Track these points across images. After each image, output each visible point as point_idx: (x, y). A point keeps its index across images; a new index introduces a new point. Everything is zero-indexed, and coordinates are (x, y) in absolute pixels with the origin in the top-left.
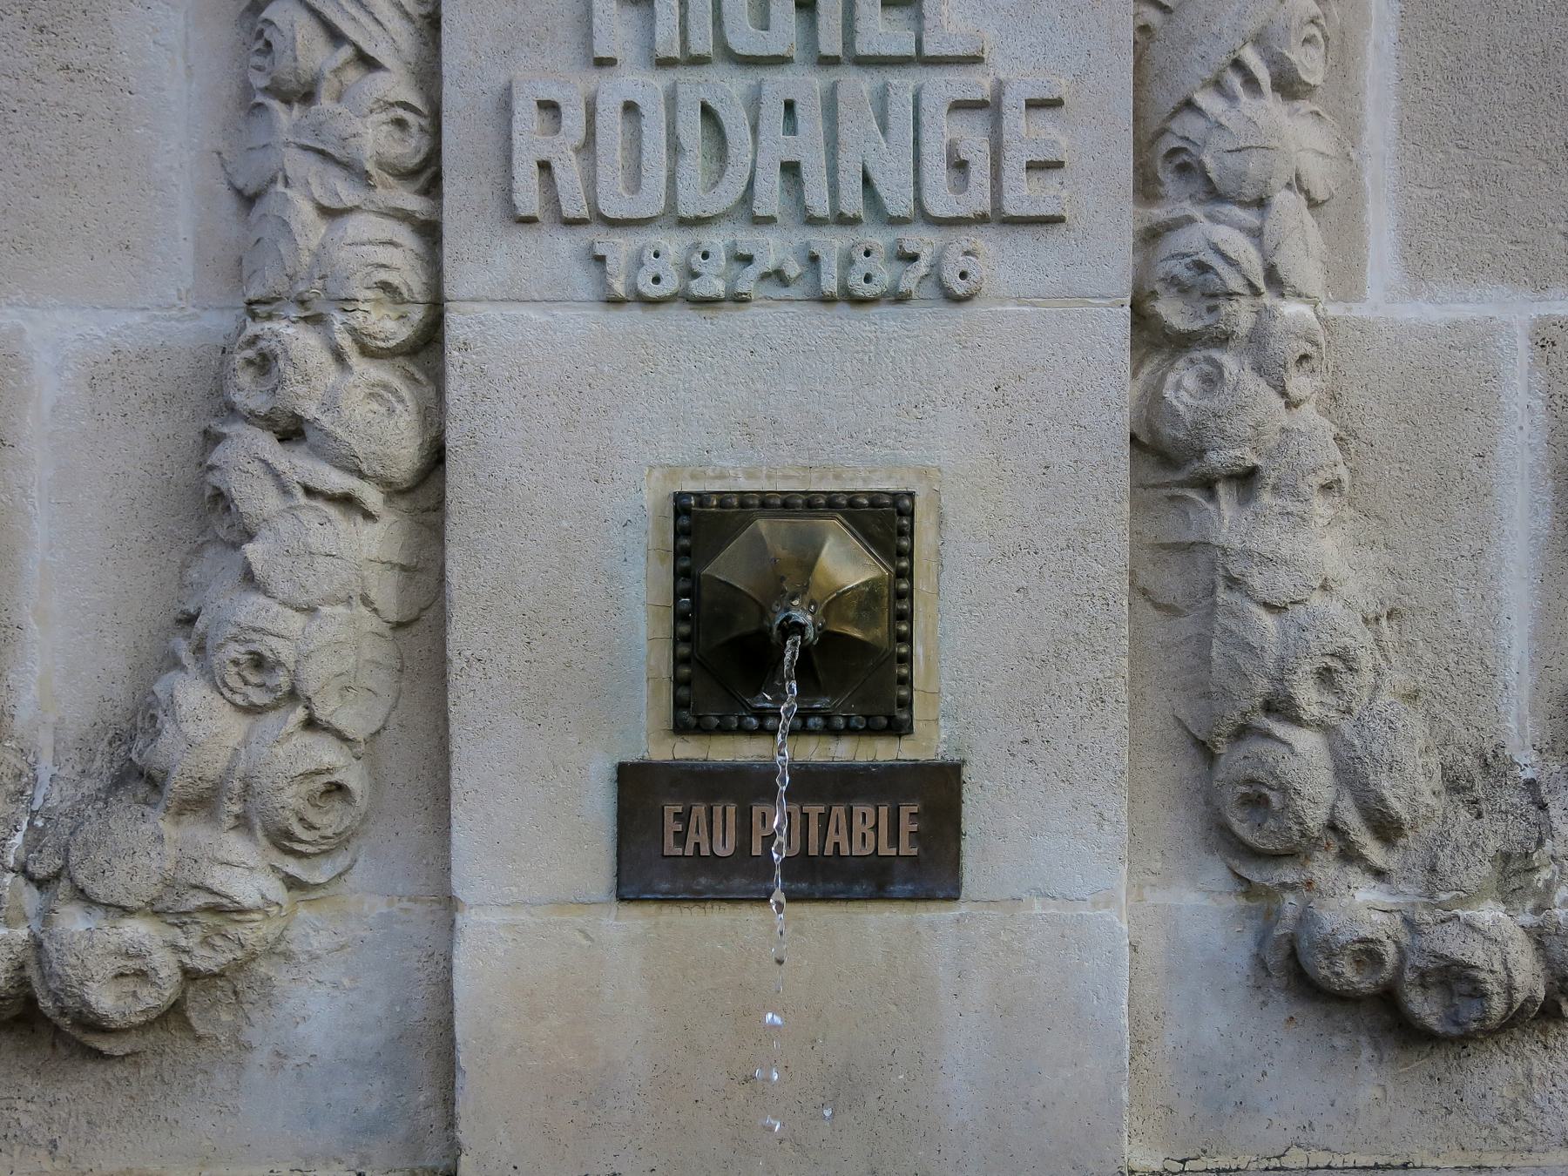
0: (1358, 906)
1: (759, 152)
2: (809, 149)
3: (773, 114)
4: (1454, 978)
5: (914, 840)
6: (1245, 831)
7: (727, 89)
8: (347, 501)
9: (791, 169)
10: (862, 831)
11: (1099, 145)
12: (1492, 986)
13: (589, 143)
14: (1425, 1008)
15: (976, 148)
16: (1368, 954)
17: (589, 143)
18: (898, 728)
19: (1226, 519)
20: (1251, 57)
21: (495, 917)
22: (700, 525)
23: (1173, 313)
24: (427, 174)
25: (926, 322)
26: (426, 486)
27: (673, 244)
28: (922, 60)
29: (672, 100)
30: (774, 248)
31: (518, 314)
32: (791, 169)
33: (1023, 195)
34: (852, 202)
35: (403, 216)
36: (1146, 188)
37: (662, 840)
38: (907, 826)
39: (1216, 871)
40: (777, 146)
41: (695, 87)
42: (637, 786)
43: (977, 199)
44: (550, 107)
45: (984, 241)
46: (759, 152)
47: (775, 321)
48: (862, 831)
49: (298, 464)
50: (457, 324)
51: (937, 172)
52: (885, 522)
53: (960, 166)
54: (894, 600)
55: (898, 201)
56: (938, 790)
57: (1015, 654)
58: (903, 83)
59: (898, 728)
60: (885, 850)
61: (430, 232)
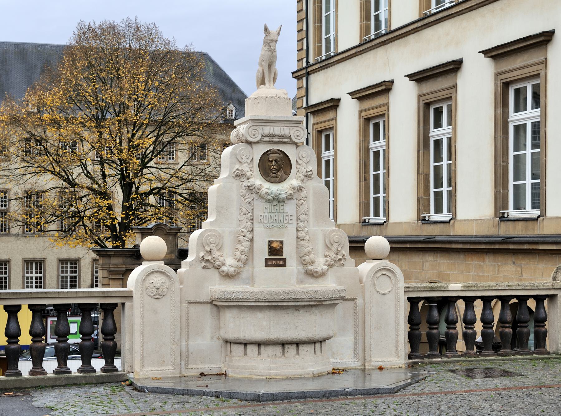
0: (311, 267)
4: (317, 272)
6: (304, 263)
7: (272, 214)
10: (280, 262)
14: (315, 274)
16: (311, 270)
18: (282, 255)
19: (302, 242)
22: (270, 243)
23: (299, 229)
24: (252, 220)
25: (284, 229)
26: (252, 240)
27: (269, 224)
30: (275, 225)
31: (259, 229)
36: (297, 220)
37: (267, 263)
39: (302, 265)
41: (270, 214)
42: (266, 260)
47: (275, 229)
48: (280, 262)
49: (244, 238)
50: (255, 229)
52: (282, 242)
54: (282, 248)
56: (285, 260)
59: (282, 255)
61: (252, 223)
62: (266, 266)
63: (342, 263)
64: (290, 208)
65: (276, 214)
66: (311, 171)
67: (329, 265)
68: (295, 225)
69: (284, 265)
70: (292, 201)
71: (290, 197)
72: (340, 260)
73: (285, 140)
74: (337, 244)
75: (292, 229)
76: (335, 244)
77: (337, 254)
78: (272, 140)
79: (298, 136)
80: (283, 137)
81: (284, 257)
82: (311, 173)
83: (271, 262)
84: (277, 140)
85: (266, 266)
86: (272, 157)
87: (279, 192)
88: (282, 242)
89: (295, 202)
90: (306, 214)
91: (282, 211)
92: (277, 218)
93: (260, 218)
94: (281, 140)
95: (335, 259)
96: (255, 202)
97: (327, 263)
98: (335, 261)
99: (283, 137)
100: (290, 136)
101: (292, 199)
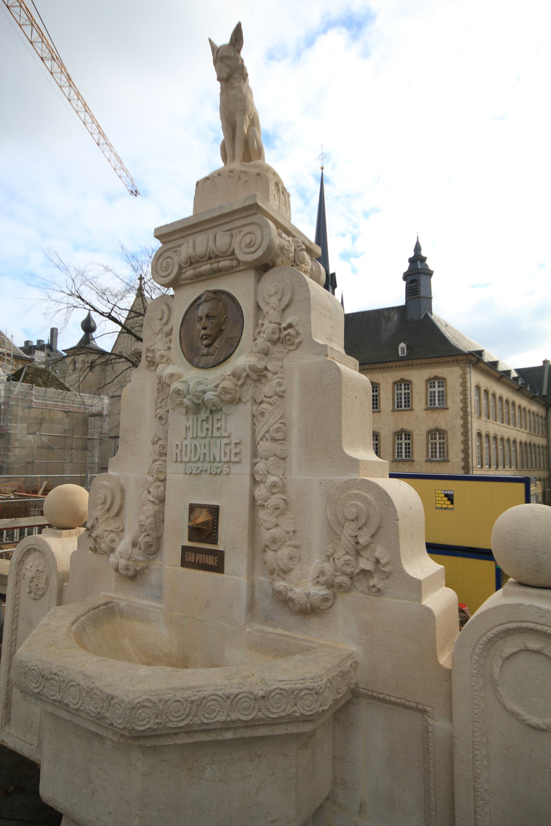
1: (201, 451)
2: (206, 451)
3: (203, 446)
5: (216, 564)
8: (153, 502)
9: (205, 454)
10: (211, 560)
11: (246, 450)
12: (297, 603)
13: (181, 451)
15: (227, 451)
17: (181, 451)
20: (267, 435)
21: (167, 567)
28: (221, 437)
29: (191, 444)
32: (205, 454)
33: (234, 459)
34: (212, 460)
35: (163, 460)
37: (189, 559)
38: (216, 561)
40: (204, 450)
42: (184, 548)
43: (227, 459)
44: (177, 445)
45: (231, 465)
46: (201, 451)
48: (211, 560)
51: (223, 455)
52: (214, 511)
53: (225, 453)
55: (218, 459)
56: (220, 555)
57: (231, 535)
58: (218, 440)
60: (213, 564)
62: (182, 565)
63: (371, 584)
64: (236, 424)
65: (206, 441)
66: (290, 326)
67: (330, 585)
68: (246, 468)
69: (218, 567)
70: (241, 408)
71: (228, 397)
72: (364, 572)
73: (224, 263)
74: (353, 525)
75: (240, 476)
76: (347, 524)
77: (358, 554)
78: (198, 270)
79: (249, 245)
80: (217, 257)
81: (220, 547)
82: (290, 330)
83: (191, 557)
84: (206, 267)
85: (182, 565)
86: (202, 311)
87: (200, 388)
88: (214, 511)
89: (246, 408)
90: (274, 440)
91: (216, 434)
92: (206, 451)
93: (175, 451)
94: (215, 266)
95: (349, 570)
96: (172, 416)
97: (322, 579)
98: (351, 576)
99: (217, 257)
100: (233, 253)
101: (236, 401)
